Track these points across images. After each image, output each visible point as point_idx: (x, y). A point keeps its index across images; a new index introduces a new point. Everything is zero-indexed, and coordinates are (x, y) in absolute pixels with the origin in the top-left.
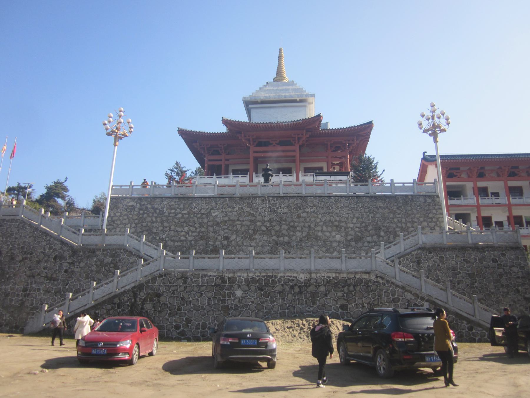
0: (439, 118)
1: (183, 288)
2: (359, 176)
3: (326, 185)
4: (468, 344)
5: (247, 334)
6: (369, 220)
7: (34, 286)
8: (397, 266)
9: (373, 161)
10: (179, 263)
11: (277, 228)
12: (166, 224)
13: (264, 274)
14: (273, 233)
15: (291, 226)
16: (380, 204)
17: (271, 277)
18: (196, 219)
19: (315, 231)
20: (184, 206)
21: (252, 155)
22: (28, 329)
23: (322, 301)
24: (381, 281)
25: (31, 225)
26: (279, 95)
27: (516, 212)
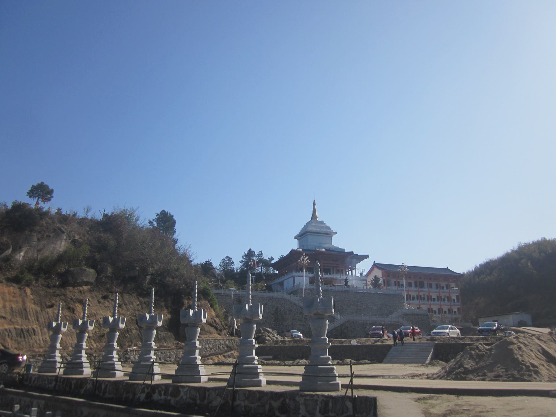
27: (410, 293)
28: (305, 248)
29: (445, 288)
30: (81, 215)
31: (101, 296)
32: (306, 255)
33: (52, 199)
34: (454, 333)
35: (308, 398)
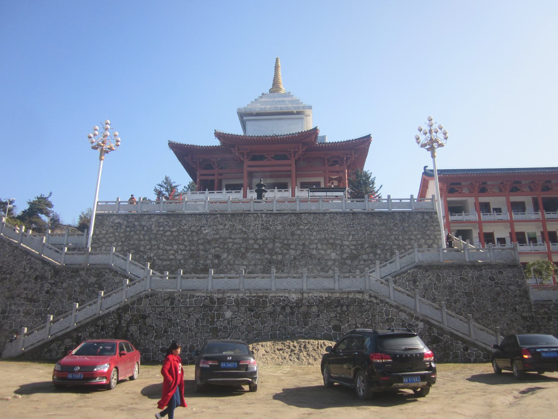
0: (436, 132)
1: (170, 310)
2: (355, 192)
3: (321, 201)
4: (462, 365)
5: (227, 356)
6: (365, 238)
7: (13, 307)
8: (392, 285)
9: (370, 177)
10: (166, 283)
11: (270, 246)
12: (154, 242)
13: (255, 295)
14: (266, 251)
15: (285, 244)
16: (377, 221)
17: (262, 297)
18: (185, 237)
19: (310, 249)
20: (173, 223)
21: (246, 170)
22: (6, 353)
23: (314, 322)
24: (375, 301)
25: (10, 243)
26: (275, 107)
27: (518, 228)
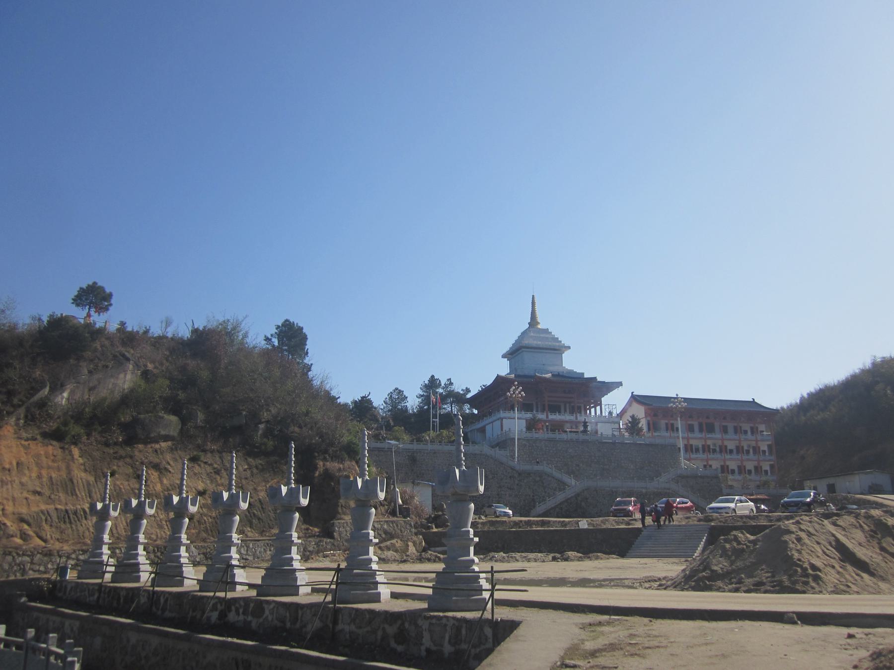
27: (692, 442)
28: (520, 373)
29: (749, 433)
30: (156, 331)
31: (188, 457)
32: (519, 385)
33: (111, 308)
34: (743, 508)
35: (434, 621)
